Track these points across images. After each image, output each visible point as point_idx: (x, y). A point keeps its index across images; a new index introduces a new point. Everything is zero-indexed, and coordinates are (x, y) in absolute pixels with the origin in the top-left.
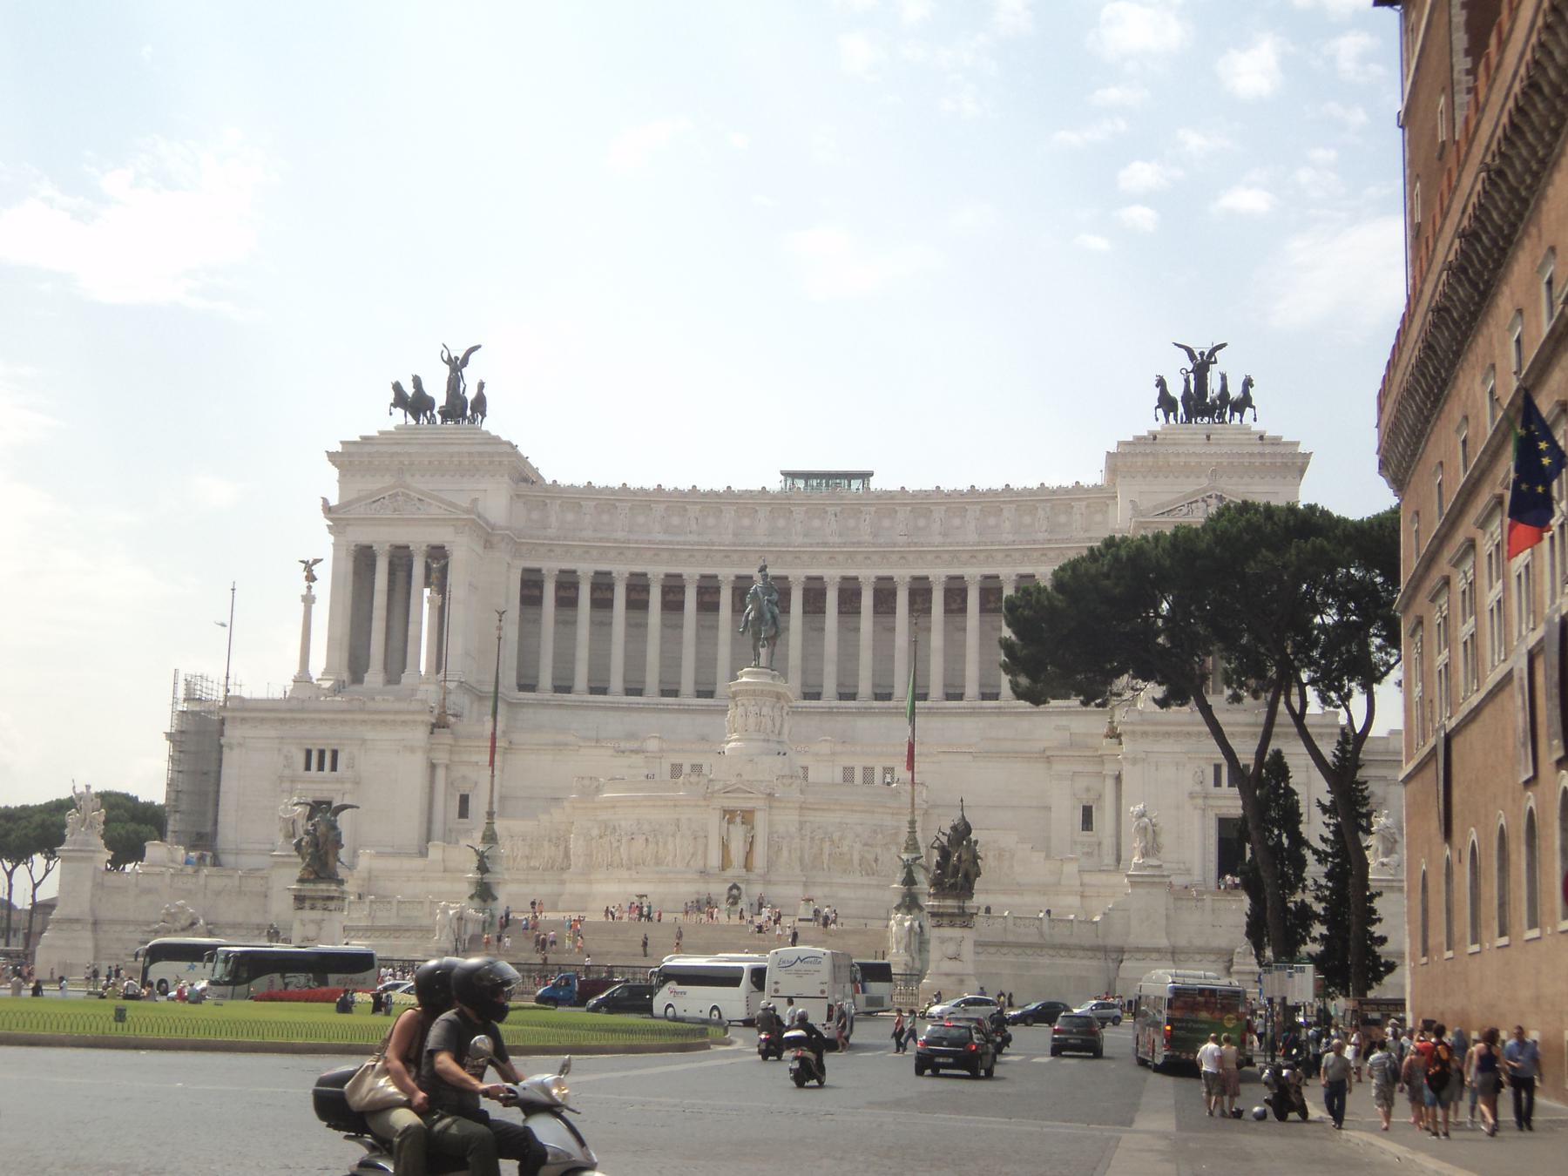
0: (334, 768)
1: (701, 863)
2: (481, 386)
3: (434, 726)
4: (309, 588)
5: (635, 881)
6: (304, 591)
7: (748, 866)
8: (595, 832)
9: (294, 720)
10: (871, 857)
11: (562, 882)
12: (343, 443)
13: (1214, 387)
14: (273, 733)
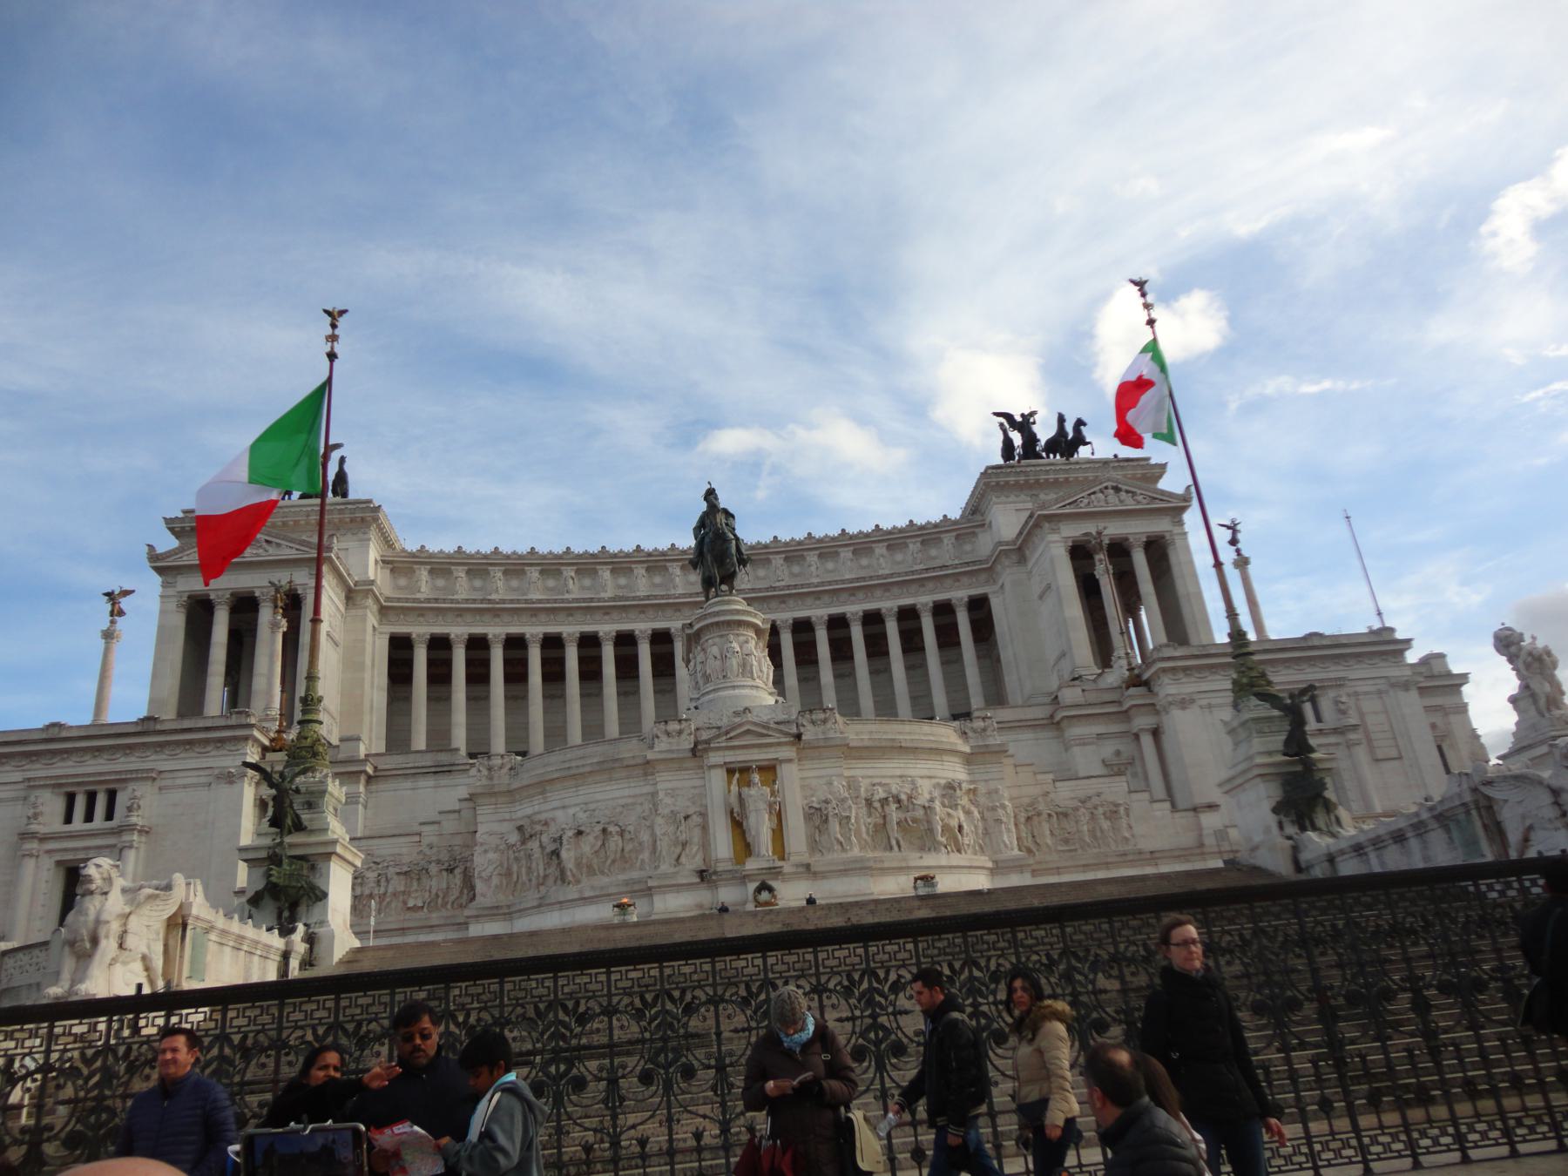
0: (109, 816)
1: (698, 863)
2: (342, 460)
3: (265, 749)
4: (113, 622)
5: (585, 900)
6: (106, 625)
7: (780, 850)
8: (514, 838)
9: (54, 753)
10: (954, 823)
11: (464, 925)
12: (184, 512)
13: (1044, 431)
14: (17, 776)
